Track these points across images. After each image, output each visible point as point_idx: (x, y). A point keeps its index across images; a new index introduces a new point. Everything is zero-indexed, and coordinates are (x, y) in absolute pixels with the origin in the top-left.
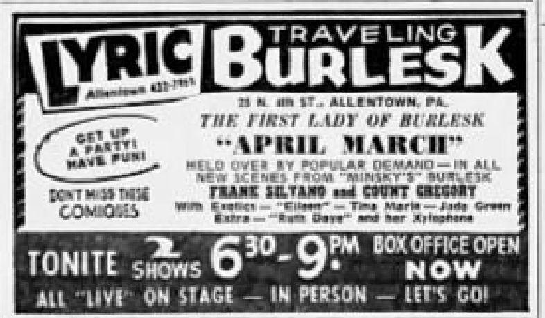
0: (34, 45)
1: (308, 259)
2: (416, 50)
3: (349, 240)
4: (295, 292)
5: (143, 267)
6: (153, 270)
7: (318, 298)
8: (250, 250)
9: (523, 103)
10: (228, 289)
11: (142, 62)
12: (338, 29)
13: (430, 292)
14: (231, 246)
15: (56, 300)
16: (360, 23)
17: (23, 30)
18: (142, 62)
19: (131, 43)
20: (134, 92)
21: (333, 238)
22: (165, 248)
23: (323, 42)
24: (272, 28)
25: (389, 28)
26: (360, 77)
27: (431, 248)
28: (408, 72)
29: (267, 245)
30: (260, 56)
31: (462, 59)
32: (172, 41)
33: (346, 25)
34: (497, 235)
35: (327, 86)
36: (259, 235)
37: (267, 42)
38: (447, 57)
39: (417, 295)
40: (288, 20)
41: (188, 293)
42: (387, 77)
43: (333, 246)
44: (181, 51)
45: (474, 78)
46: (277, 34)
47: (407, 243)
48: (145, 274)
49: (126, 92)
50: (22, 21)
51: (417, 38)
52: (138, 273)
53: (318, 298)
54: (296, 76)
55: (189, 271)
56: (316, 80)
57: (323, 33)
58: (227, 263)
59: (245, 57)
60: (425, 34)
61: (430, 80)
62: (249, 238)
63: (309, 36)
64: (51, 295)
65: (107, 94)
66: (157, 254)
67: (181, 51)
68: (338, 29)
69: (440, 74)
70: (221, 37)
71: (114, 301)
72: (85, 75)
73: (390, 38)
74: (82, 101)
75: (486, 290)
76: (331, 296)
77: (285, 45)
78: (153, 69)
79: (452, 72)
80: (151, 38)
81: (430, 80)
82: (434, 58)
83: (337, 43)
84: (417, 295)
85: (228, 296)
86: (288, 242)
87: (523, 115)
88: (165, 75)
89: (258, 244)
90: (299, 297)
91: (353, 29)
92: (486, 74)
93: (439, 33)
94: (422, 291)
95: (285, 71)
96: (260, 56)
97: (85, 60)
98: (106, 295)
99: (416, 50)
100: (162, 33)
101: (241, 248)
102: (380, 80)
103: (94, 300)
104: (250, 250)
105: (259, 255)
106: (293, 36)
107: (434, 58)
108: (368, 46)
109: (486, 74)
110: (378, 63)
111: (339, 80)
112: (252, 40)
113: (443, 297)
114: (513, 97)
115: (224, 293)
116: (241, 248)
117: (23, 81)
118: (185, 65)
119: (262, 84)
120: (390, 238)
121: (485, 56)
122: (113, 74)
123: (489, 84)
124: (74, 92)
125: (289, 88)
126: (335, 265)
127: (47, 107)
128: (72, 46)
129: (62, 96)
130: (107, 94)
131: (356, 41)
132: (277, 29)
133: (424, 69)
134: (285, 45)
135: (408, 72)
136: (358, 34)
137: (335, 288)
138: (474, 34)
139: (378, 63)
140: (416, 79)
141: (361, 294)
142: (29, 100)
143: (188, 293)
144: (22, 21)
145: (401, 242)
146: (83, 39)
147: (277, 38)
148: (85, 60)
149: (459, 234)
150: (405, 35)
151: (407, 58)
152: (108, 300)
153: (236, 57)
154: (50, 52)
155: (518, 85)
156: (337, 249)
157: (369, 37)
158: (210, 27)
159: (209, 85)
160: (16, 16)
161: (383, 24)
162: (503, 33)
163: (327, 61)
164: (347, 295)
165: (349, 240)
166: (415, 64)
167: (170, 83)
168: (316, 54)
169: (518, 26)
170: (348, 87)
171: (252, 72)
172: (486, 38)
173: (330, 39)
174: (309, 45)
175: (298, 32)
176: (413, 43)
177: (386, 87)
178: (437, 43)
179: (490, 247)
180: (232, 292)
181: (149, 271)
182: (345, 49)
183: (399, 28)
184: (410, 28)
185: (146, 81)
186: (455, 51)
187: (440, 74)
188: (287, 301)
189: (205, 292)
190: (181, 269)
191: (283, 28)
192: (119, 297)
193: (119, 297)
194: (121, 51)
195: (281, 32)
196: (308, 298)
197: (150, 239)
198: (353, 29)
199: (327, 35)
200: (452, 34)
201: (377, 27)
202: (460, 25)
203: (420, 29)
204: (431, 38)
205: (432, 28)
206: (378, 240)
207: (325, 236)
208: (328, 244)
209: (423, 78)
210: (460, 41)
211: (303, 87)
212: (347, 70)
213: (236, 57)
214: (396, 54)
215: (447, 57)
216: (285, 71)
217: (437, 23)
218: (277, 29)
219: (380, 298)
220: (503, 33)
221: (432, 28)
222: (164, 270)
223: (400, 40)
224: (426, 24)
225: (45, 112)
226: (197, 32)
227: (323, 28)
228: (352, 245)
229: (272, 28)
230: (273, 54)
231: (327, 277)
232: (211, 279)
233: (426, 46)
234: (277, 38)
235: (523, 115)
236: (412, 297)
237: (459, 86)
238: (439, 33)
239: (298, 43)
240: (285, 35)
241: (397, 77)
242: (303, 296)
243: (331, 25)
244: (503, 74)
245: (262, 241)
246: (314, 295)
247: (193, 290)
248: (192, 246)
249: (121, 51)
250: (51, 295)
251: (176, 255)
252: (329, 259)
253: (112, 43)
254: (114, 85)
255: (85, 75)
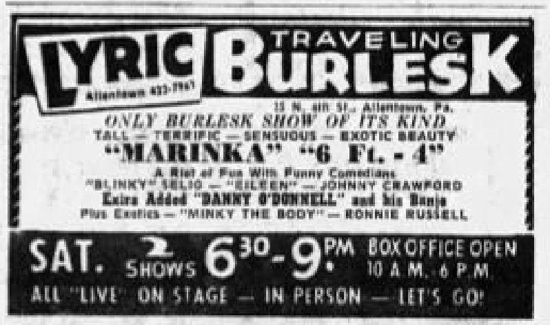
0: (33, 46)
1: (300, 260)
2: (420, 57)
3: (344, 242)
4: (289, 293)
5: (137, 266)
6: (146, 270)
7: (312, 298)
8: (244, 250)
9: (530, 113)
10: (222, 290)
11: (142, 65)
12: (342, 34)
13: (425, 295)
14: (223, 247)
15: (51, 295)
16: (364, 30)
17: (20, 33)
18: (142, 65)
19: (131, 46)
20: (133, 95)
21: (327, 240)
22: (159, 248)
23: (326, 48)
24: (273, 33)
25: (393, 35)
26: (364, 83)
27: (426, 251)
28: (411, 79)
29: (261, 246)
30: (262, 60)
31: (468, 68)
32: (174, 43)
33: (350, 31)
34: (493, 239)
35: (330, 91)
36: (253, 236)
37: (269, 46)
38: (452, 64)
39: (411, 296)
40: (290, 25)
41: (182, 293)
42: (390, 84)
43: (327, 248)
44: (182, 54)
45: (480, 85)
46: (279, 37)
47: (401, 247)
48: (139, 273)
49: (124, 95)
50: (21, 21)
51: (422, 44)
52: (131, 272)
53: (312, 298)
54: (298, 81)
55: (185, 271)
56: (319, 85)
57: (326, 38)
58: (221, 264)
59: (246, 60)
60: (429, 40)
61: (434, 87)
62: (243, 238)
63: (314, 40)
64: (46, 290)
65: (105, 96)
66: (153, 253)
67: (182, 54)
68: (342, 34)
69: (445, 82)
70: (223, 41)
71: (108, 296)
72: (84, 77)
73: (394, 45)
74: (81, 102)
75: (482, 294)
76: (325, 296)
77: (287, 50)
78: (153, 72)
79: (458, 79)
80: (151, 42)
81: (434, 87)
82: (439, 65)
83: (341, 48)
84: (411, 296)
85: (222, 296)
86: (282, 242)
87: (530, 124)
88: (165, 78)
89: (252, 245)
90: (292, 298)
91: (357, 35)
92: (493, 82)
93: (445, 40)
94: (416, 295)
95: (287, 74)
96: (262, 60)
97: (84, 62)
98: (100, 295)
99: (420, 57)
100: (163, 37)
101: (236, 248)
102: (381, 87)
103: (88, 297)
104: (244, 250)
105: (253, 252)
106: (296, 42)
107: (439, 65)
108: (373, 53)
109: (493, 82)
110: (382, 70)
111: (342, 86)
112: (255, 45)
113: (438, 299)
114: (521, 107)
115: (218, 293)
116: (236, 248)
117: (21, 83)
118: (186, 69)
119: (263, 90)
120: (385, 240)
121: (491, 63)
122: (112, 76)
123: (496, 92)
124: (72, 93)
125: (289, 94)
126: (330, 266)
127: (45, 108)
128: (71, 47)
129: (60, 98)
130: (105, 96)
131: (360, 46)
132: (279, 35)
133: (428, 76)
134: (287, 50)
135: (411, 79)
136: (362, 40)
137: (329, 290)
138: (481, 42)
139: (382, 70)
140: (420, 86)
141: (354, 296)
142: (27, 102)
143: (182, 293)
144: (21, 21)
145: (396, 245)
146: (82, 40)
147: (279, 43)
148: (84, 62)
149: (454, 238)
150: (410, 42)
151: (411, 64)
152: (102, 298)
153: (239, 61)
154: (49, 54)
155: (526, 93)
156: (333, 251)
157: (373, 43)
158: (212, 31)
159: (210, 89)
160: (15, 17)
161: (387, 31)
162: (512, 41)
163: (330, 66)
164: (342, 296)
165: (344, 242)
166: (420, 71)
167: (170, 85)
168: (319, 60)
169: (526, 33)
170: (352, 94)
171: (252, 79)
172: (493, 47)
173: (334, 44)
174: (312, 50)
175: (301, 37)
176: (417, 50)
177: (390, 94)
178: (442, 50)
179: (486, 250)
180: (225, 292)
181: (143, 270)
182: (349, 55)
183: (403, 34)
184: (414, 35)
185: (145, 83)
186: (462, 58)
187: (445, 82)
188: (281, 301)
189: (199, 292)
190: (174, 269)
191: (286, 33)
192: (113, 295)
193: (113, 295)
194: (120, 53)
195: (284, 38)
196: (302, 299)
197: (145, 239)
198: (357, 35)
199: (331, 41)
200: (459, 41)
201: (381, 33)
202: (467, 33)
203: (425, 37)
204: (436, 45)
205: (437, 36)
206: (372, 243)
207: (320, 238)
208: (322, 246)
209: (427, 85)
210: (467, 48)
211: (307, 93)
212: (350, 76)
213: (239, 61)
214: (400, 61)
215: (452, 64)
216: (287, 74)
217: (442, 31)
218: (279, 35)
219: (374, 298)
220: (512, 41)
221: (437, 36)
222: (159, 269)
223: (404, 46)
224: (431, 31)
225: (43, 113)
226: (199, 35)
227: (327, 33)
228: (347, 247)
229: (273, 33)
230: (275, 59)
231: (322, 277)
232: (203, 278)
233: (431, 53)
234: (279, 43)
235: (530, 124)
236: (406, 298)
237: (464, 94)
238: (445, 40)
239: (301, 48)
240: (287, 40)
241: (401, 85)
242: (296, 296)
243: (335, 31)
244: (511, 82)
245: (257, 241)
246: (308, 296)
247: (187, 290)
248: (187, 247)
249: (120, 53)
250: (46, 290)
251: (171, 254)
252: (324, 259)
253: (112, 45)
254: (113, 87)
255: (84, 77)
